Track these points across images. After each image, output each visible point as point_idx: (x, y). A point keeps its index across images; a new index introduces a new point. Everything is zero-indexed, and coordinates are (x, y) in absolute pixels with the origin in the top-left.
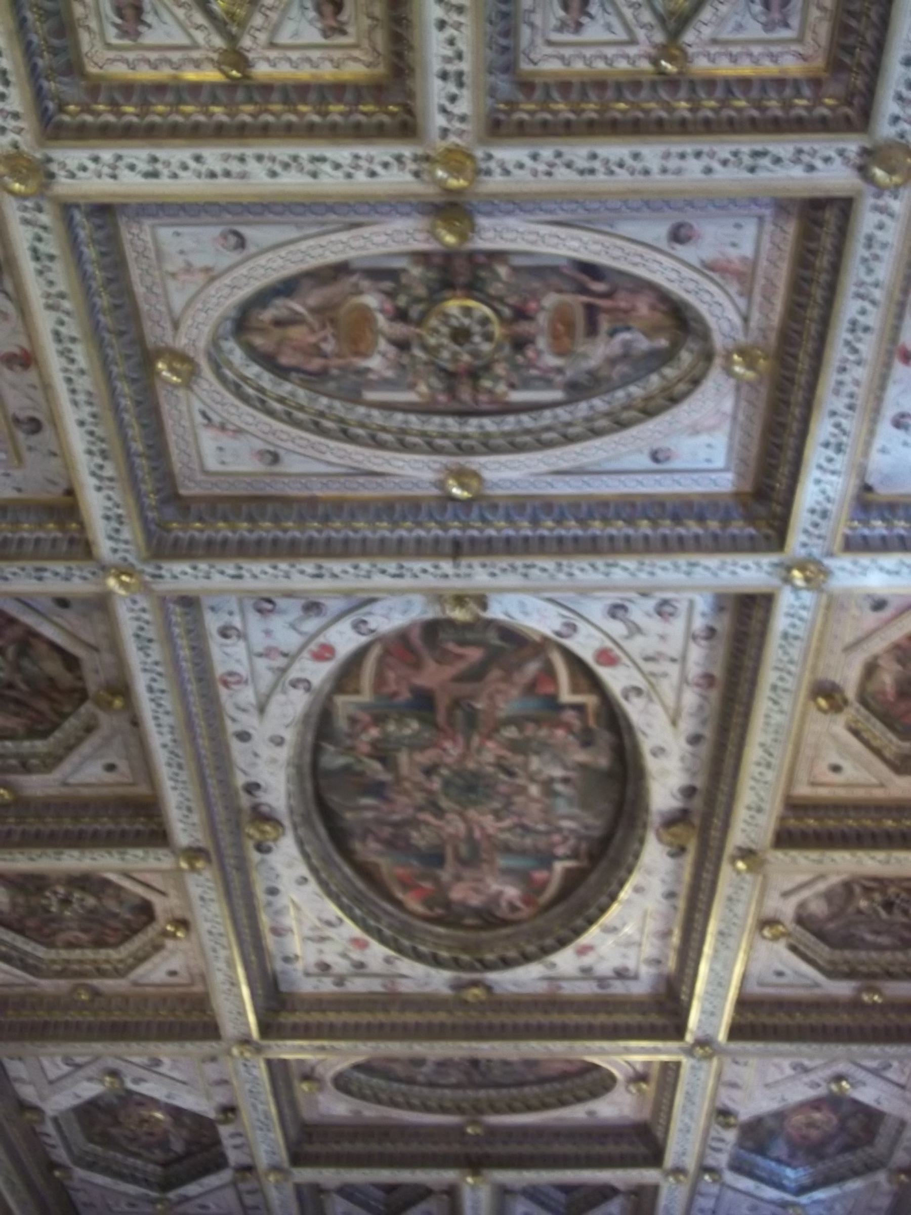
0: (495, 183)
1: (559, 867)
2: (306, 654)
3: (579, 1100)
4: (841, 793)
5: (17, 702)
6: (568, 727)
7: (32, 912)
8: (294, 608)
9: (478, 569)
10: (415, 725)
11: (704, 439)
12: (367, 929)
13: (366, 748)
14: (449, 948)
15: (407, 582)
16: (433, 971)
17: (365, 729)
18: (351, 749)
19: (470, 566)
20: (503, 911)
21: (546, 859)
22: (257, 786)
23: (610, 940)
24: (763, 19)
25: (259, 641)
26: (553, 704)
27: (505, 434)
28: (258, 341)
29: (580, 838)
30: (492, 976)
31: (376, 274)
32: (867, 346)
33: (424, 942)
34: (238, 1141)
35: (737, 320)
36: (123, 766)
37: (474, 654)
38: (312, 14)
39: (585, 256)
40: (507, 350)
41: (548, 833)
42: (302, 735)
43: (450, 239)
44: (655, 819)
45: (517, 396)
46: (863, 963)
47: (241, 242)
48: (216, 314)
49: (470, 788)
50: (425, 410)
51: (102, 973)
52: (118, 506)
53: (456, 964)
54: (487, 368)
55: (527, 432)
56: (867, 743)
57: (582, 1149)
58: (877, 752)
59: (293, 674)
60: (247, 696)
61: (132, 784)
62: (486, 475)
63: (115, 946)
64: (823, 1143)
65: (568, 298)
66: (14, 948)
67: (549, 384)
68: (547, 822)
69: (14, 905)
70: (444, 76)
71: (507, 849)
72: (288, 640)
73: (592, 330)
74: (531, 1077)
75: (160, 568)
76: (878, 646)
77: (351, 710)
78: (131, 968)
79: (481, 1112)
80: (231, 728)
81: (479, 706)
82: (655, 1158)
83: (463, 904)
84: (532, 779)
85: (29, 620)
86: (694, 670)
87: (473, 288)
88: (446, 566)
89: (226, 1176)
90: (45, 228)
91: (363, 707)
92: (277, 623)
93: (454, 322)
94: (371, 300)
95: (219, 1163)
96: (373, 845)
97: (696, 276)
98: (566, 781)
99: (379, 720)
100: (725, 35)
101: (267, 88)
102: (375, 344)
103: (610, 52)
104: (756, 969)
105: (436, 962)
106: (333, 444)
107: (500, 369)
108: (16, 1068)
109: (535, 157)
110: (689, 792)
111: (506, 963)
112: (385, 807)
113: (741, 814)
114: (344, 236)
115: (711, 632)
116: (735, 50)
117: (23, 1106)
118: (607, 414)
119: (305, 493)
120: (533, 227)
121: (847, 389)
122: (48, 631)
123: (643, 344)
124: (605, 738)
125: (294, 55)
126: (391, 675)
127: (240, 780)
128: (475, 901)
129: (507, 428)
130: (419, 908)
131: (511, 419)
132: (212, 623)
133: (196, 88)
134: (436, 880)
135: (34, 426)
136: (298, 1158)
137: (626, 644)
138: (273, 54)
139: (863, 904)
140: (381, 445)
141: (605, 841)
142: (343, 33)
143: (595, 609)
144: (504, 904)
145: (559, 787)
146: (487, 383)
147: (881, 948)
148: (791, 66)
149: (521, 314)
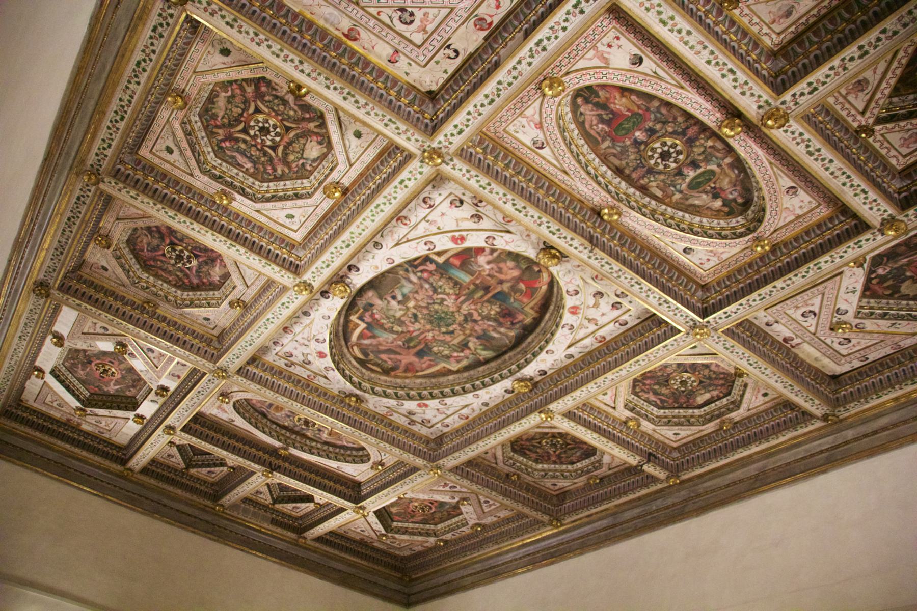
6: (372, 315)
10: (435, 349)
26: (369, 327)
41: (426, 281)
49: (441, 318)
68: (422, 287)
71: (456, 283)
81: (400, 343)
84: (408, 308)
98: (394, 298)
145: (400, 298)
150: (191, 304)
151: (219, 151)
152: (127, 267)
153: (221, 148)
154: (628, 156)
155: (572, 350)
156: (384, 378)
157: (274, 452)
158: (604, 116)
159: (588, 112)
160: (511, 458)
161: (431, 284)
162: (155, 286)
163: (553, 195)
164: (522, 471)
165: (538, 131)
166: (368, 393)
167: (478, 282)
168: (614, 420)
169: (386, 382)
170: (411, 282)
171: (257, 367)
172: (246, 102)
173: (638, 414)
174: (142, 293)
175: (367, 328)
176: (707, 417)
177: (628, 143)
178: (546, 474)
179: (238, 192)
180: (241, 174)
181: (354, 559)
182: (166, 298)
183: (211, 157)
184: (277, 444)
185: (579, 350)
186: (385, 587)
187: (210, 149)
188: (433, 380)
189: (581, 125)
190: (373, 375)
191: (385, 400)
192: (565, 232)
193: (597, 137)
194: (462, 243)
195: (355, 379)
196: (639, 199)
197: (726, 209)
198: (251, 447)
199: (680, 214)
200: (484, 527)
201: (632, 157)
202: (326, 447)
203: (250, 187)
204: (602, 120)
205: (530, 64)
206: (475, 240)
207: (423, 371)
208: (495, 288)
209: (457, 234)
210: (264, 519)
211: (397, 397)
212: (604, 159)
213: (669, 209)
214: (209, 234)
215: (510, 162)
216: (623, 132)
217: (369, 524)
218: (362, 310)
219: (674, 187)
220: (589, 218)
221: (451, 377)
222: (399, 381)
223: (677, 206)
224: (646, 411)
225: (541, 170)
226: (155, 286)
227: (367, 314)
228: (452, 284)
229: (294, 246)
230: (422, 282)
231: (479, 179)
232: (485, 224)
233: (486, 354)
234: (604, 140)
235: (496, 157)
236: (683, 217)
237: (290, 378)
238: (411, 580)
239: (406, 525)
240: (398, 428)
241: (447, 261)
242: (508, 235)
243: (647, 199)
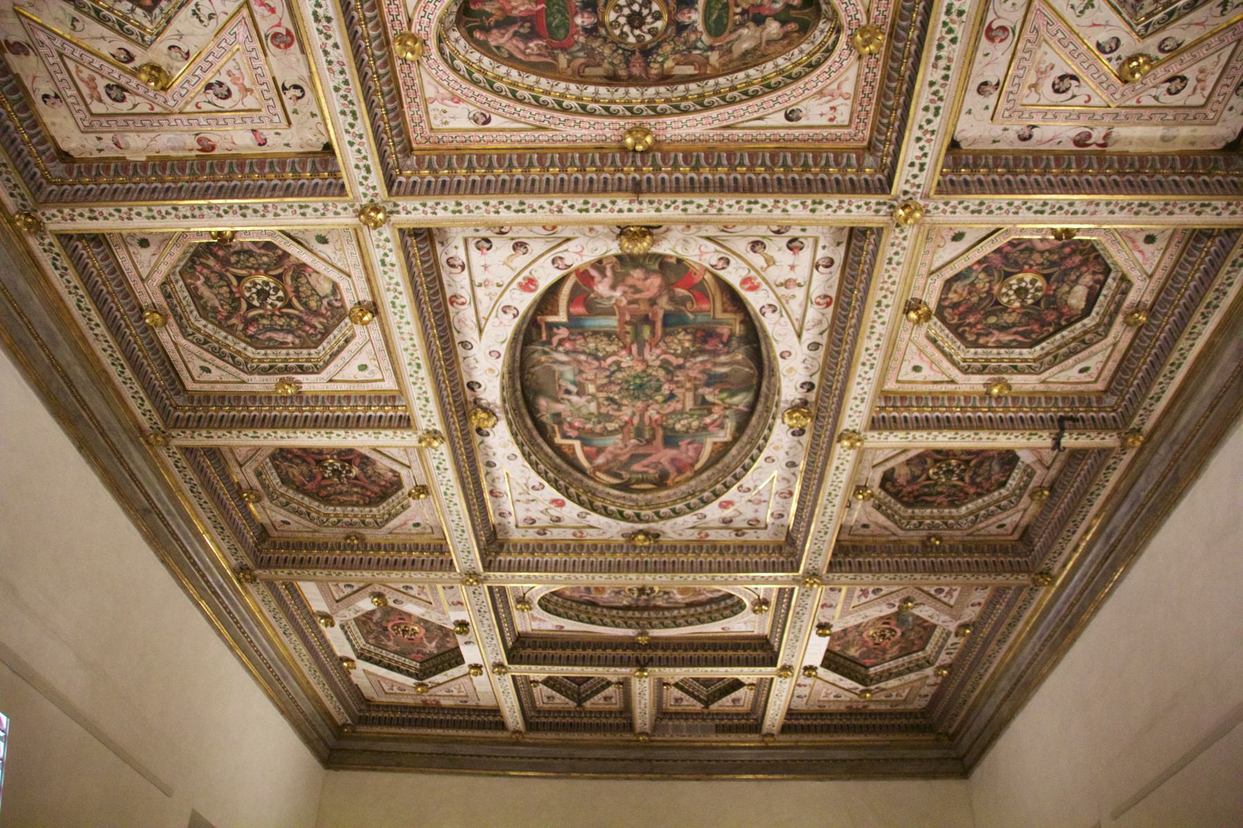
6: (571, 426)
10: (678, 426)
17: (714, 422)
18: (729, 407)
21: (574, 324)
26: (585, 443)
29: (549, 342)
41: (575, 351)
49: (641, 386)
68: (579, 362)
71: (609, 335)
77: (722, 433)
81: (633, 441)
91: (712, 434)
96: (725, 331)
98: (568, 392)
99: (705, 428)
112: (709, 366)
124: (546, 418)
126: (691, 453)
134: (672, 299)
144: (609, 273)
145: (574, 389)
150: (392, 516)
151: (253, 341)
152: (304, 510)
153: (251, 337)
154: (601, 54)
155: (808, 337)
156: (664, 493)
157: (631, 644)
158: (522, 31)
159: (502, 41)
160: (912, 518)
161: (584, 352)
162: (346, 516)
163: (552, 164)
164: (937, 527)
165: (462, 105)
166: (653, 521)
167: (628, 318)
168: (967, 399)
169: (669, 497)
170: (563, 363)
171: (509, 552)
172: (222, 277)
173: (997, 371)
174: (337, 530)
176: (1106, 320)
177: (582, 39)
178: (977, 517)
179: (297, 373)
180: (291, 351)
181: (856, 738)
182: (363, 522)
183: (250, 352)
184: (630, 632)
185: (816, 331)
186: (920, 760)
187: (243, 345)
188: (719, 466)
189: (511, 60)
190: (649, 496)
191: (680, 520)
192: (597, 200)
193: (542, 59)
194: (537, 286)
195: (628, 512)
196: (669, 95)
197: (792, 26)
198: (605, 649)
199: (741, 75)
200: (974, 625)
201: (607, 52)
202: (692, 611)
203: (308, 360)
204: (527, 38)
205: (336, 46)
206: (546, 276)
207: (697, 461)
208: (655, 314)
209: (520, 279)
210: (705, 730)
211: (691, 508)
212: (580, 78)
213: (721, 80)
214: (299, 433)
215: (470, 161)
216: (562, 32)
217: (833, 684)
218: (556, 427)
219: (696, 48)
220: (622, 161)
221: (734, 451)
222: (683, 488)
223: (728, 68)
224: (1012, 360)
225: (517, 145)
226: (346, 516)
227: (566, 427)
228: (605, 339)
229: (394, 398)
230: (573, 355)
231: (442, 205)
232: (536, 247)
233: (741, 400)
234: (555, 58)
235: (450, 167)
236: (748, 76)
237: (554, 547)
238: (952, 737)
239: (886, 666)
240: (728, 547)
241: (569, 315)
242: (570, 243)
243: (681, 87)
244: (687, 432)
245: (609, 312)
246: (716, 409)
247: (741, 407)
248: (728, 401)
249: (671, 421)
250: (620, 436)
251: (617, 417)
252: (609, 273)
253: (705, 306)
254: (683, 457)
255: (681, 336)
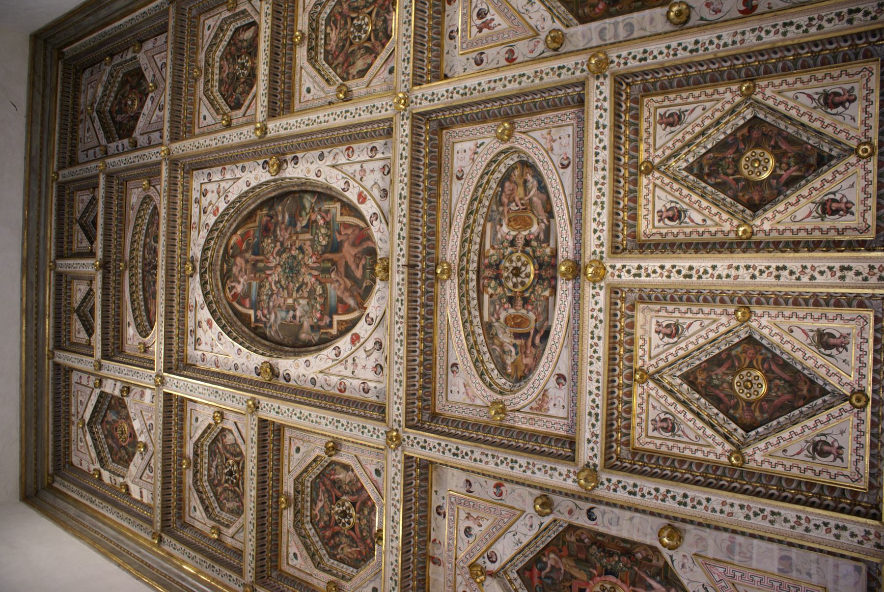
0: (589, 290)
1: (252, 312)
2: (361, 189)
3: (135, 319)
4: (286, 453)
5: (344, 46)
7: (238, 50)
8: (384, 184)
9: (402, 276)
10: (324, 243)
11: (462, 390)
12: (222, 215)
13: (313, 218)
14: (212, 256)
15: (396, 241)
16: (201, 248)
17: (323, 218)
18: (313, 209)
19: (403, 273)
20: (229, 284)
21: (255, 306)
22: (296, 164)
23: (215, 337)
24: (658, 419)
25: (368, 166)
26: (333, 312)
27: (467, 291)
28: (517, 172)
29: (265, 323)
30: (198, 277)
31: (547, 231)
32: (504, 469)
33: (215, 243)
34: (120, 148)
35: (518, 407)
36: (309, 96)
37: (359, 274)
38: (668, 206)
39: (552, 332)
40: (509, 294)
41: (268, 308)
42: (321, 186)
43: (563, 268)
44: (273, 361)
45: (486, 297)
46: (202, 460)
47: (564, 167)
48: (530, 152)
49: (291, 269)
50: (481, 253)
51: (206, 83)
52: (439, 99)
53: (204, 260)
54: (501, 284)
55: (469, 303)
56: (310, 465)
57: (111, 320)
58: (306, 470)
59: (351, 182)
60: (342, 159)
61: (300, 102)
62: (448, 282)
63: (220, 91)
64: (113, 438)
65: (533, 325)
66: (221, 41)
67: (491, 314)
68: (274, 306)
69: (242, 41)
70: (639, 267)
71: (260, 287)
72: (368, 182)
73: (517, 336)
74: (147, 295)
75: (407, 118)
76: (358, 471)
77: (333, 211)
78: (208, 98)
79: (130, 270)
80: (326, 151)
81: (333, 275)
82: (106, 356)
83: (235, 264)
84: (295, 300)
85: (384, 55)
86: (347, 382)
87: (539, 277)
88: (403, 261)
89: (104, 142)
90: (573, 73)
92: (378, 175)
93: (523, 268)
94: (535, 228)
95: (109, 139)
96: (265, 219)
97: (540, 387)
98: (294, 317)
99: (327, 224)
100: (651, 400)
101: (635, 183)
102: (514, 230)
103: (646, 347)
104: (198, 407)
105: (205, 250)
106: (466, 207)
107: (499, 290)
108: (161, 39)
109: (600, 310)
110: (287, 378)
111: (204, 284)
112: (283, 226)
113: (276, 404)
114: (566, 217)
115: (366, 391)
116: (644, 406)
117: (141, 42)
118: (476, 342)
119: (442, 192)
120: (567, 309)
121: (484, 458)
122: (379, 62)
123: (509, 361)
124: (316, 338)
125: (650, 197)
126: (349, 231)
127: (299, 155)
128: (235, 270)
129: (471, 292)
130: (232, 242)
131: (475, 295)
132: (379, 143)
133: (636, 149)
134: (246, 251)
135: (479, 62)
136: (110, 177)
137: (361, 350)
138: (651, 187)
139: (231, 461)
140: (464, 231)
141: (264, 337)
142: (659, 221)
143: (378, 335)
144: (233, 284)
145: (291, 313)
146: (493, 283)
147: (209, 470)
148: (636, 432)
149: (526, 301)
161: (268, 303)
170: (276, 316)
175: (337, 313)
207: (358, 226)
208: (252, 260)
227: (322, 324)
241: (251, 308)
244: (329, 236)
245: (250, 285)
246: (313, 218)
247: (313, 201)
248: (308, 210)
249: (319, 248)
250: (328, 285)
251: (312, 285)
252: (233, 284)
253: (252, 233)
254: (352, 237)
255: (265, 245)
